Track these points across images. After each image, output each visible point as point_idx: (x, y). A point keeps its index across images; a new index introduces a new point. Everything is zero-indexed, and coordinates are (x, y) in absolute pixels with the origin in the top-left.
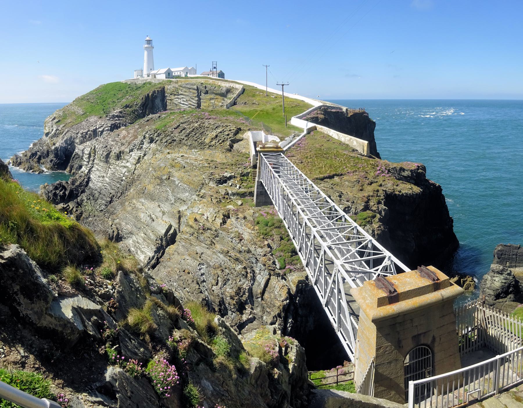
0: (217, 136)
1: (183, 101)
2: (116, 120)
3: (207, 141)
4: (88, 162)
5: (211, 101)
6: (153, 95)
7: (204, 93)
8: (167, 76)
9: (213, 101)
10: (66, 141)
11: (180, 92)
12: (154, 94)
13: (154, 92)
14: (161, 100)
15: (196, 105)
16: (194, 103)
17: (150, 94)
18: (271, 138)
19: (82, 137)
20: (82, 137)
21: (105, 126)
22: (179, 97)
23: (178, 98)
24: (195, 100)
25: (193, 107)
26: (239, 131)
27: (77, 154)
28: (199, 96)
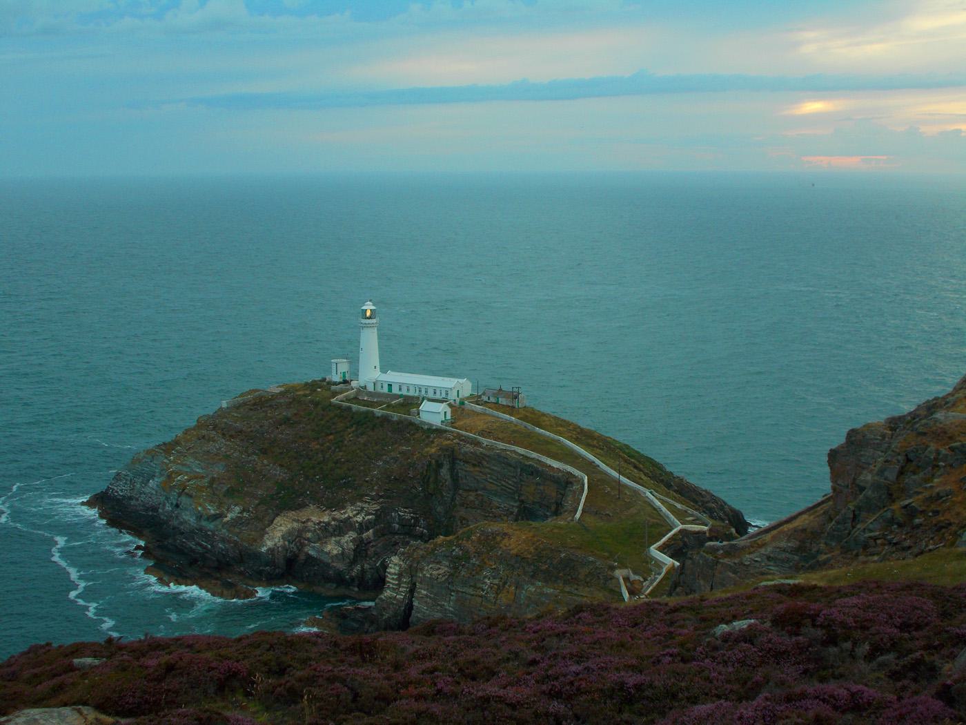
0: (589, 572)
1: (490, 478)
4: (399, 585)
9: (542, 488)
16: (510, 484)
17: (433, 461)
18: (637, 577)
24: (513, 481)
25: (510, 491)
27: (309, 557)
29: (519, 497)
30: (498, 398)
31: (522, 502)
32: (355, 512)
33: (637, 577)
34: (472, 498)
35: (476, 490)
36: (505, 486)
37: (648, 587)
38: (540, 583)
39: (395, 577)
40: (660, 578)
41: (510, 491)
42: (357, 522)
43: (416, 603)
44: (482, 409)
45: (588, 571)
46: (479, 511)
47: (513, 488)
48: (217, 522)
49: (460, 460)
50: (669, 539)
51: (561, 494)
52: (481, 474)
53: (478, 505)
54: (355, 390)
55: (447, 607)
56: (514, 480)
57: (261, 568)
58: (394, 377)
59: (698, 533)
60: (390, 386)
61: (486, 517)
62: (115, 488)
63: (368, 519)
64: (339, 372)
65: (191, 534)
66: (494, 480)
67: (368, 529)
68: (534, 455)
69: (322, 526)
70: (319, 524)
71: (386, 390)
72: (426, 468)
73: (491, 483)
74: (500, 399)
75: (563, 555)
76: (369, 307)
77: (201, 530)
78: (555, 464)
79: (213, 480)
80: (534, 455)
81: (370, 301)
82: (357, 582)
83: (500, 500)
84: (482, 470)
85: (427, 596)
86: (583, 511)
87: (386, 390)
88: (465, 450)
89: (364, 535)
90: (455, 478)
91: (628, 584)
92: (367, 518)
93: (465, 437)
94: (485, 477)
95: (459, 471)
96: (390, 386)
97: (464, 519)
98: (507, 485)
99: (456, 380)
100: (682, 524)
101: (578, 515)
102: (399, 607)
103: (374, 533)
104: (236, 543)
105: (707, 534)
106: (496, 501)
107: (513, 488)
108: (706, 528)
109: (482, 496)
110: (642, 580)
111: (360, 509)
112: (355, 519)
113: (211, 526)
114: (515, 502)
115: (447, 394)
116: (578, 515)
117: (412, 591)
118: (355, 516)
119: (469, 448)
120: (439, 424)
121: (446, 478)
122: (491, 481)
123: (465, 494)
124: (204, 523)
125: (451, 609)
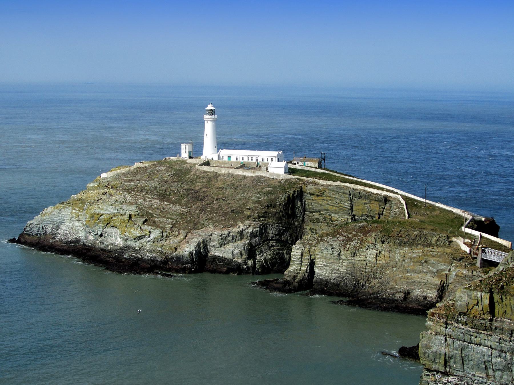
2: (262, 220)
3: (433, 242)
4: (301, 261)
5: (366, 205)
6: (293, 195)
9: (368, 205)
10: (199, 245)
11: (325, 193)
13: (294, 192)
15: (350, 208)
17: (291, 194)
19: (222, 239)
20: (222, 239)
21: (252, 227)
22: (325, 198)
26: (448, 237)
28: (351, 200)
31: (354, 216)
32: (245, 227)
35: (320, 211)
36: (342, 206)
38: (407, 248)
39: (299, 257)
42: (248, 232)
43: (317, 271)
46: (323, 224)
48: (142, 241)
51: (382, 208)
52: (323, 201)
55: (342, 270)
57: (184, 265)
58: (225, 153)
61: (329, 226)
62: (31, 233)
65: (122, 250)
69: (224, 237)
70: (220, 236)
76: (210, 107)
77: (127, 247)
79: (130, 217)
81: (211, 103)
82: (251, 271)
83: (338, 216)
84: (325, 198)
85: (324, 265)
87: (226, 159)
90: (303, 205)
92: (254, 230)
94: (326, 202)
95: (306, 200)
97: (313, 229)
98: (343, 205)
99: (278, 152)
102: (305, 274)
103: (258, 239)
104: (162, 253)
106: (334, 216)
108: (483, 219)
109: (325, 214)
112: (247, 231)
113: (136, 245)
117: (312, 264)
118: (247, 228)
123: (311, 214)
124: (129, 243)
125: (344, 271)
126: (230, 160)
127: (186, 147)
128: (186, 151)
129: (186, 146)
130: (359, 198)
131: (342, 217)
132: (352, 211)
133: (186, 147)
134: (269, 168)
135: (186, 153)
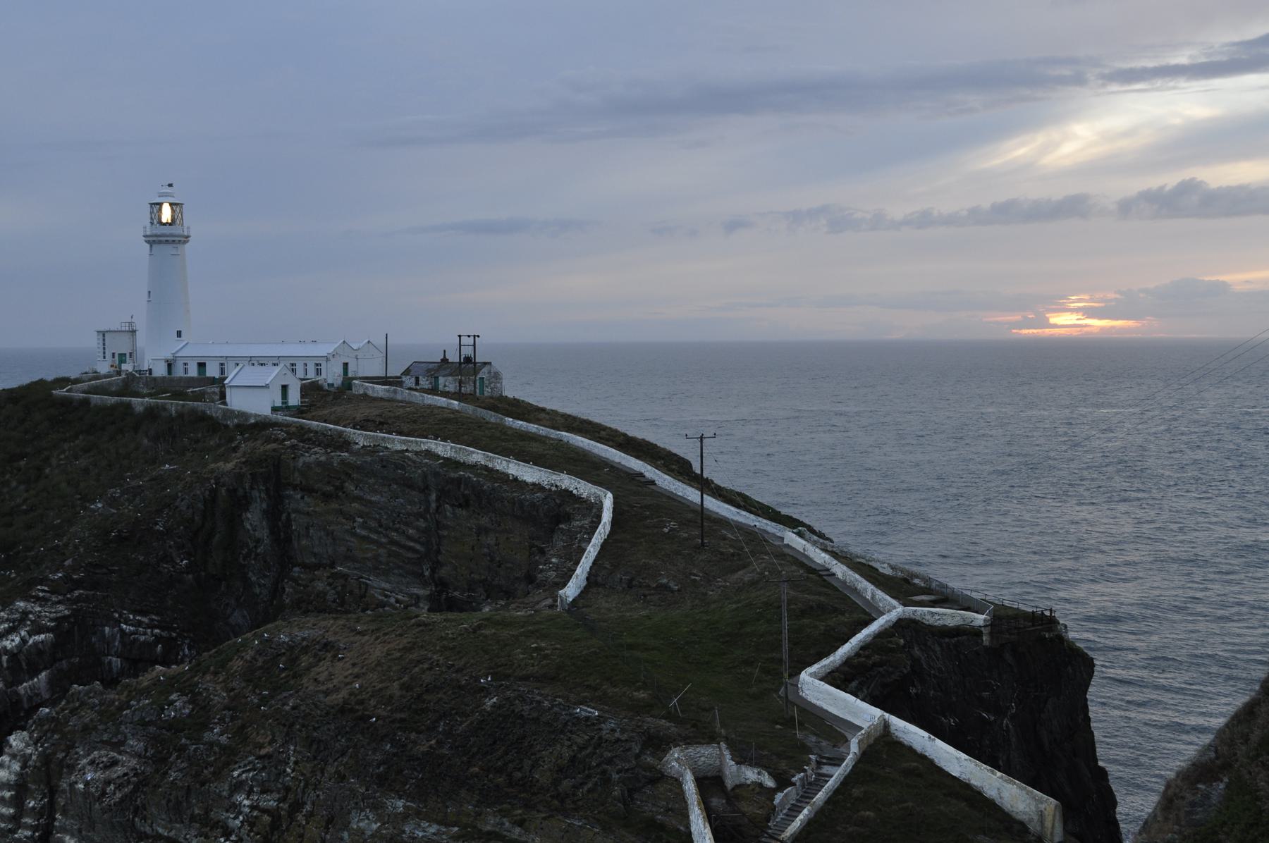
0: (573, 759)
1: (364, 526)
7: (452, 505)
8: (279, 403)
9: (491, 540)
11: (350, 487)
12: (235, 490)
14: (265, 512)
16: (410, 538)
18: (751, 775)
23: (341, 512)
24: (417, 529)
25: (410, 555)
29: (433, 571)
30: (436, 378)
31: (442, 585)
33: (751, 775)
34: (320, 586)
35: (333, 565)
37: (796, 810)
40: (837, 774)
41: (410, 555)
44: (388, 391)
45: (567, 754)
47: (418, 547)
49: (295, 488)
50: (862, 648)
53: (334, 601)
54: (123, 376)
56: (422, 524)
59: (958, 631)
60: (202, 366)
63: (35, 644)
64: (108, 355)
66: (370, 529)
67: (34, 672)
68: (477, 456)
71: (193, 372)
72: (200, 506)
73: (364, 538)
74: (441, 380)
75: (490, 702)
78: (529, 474)
80: (477, 456)
83: (387, 586)
86: (591, 578)
87: (193, 372)
88: (307, 460)
89: (23, 688)
90: (282, 536)
91: (716, 802)
93: (316, 432)
95: (293, 516)
96: (202, 366)
98: (403, 541)
100: (905, 605)
101: (571, 591)
105: (986, 639)
107: (418, 547)
110: (770, 783)
111: (17, 616)
114: (425, 584)
115: (318, 372)
116: (571, 591)
119: (316, 455)
120: (267, 412)
121: (257, 535)
122: (364, 533)
126: (205, 374)
127: (104, 340)
128: (104, 353)
129: (104, 335)
130: (460, 506)
131: (401, 591)
132: (436, 566)
133: (104, 340)
134: (228, 391)
135: (104, 357)
